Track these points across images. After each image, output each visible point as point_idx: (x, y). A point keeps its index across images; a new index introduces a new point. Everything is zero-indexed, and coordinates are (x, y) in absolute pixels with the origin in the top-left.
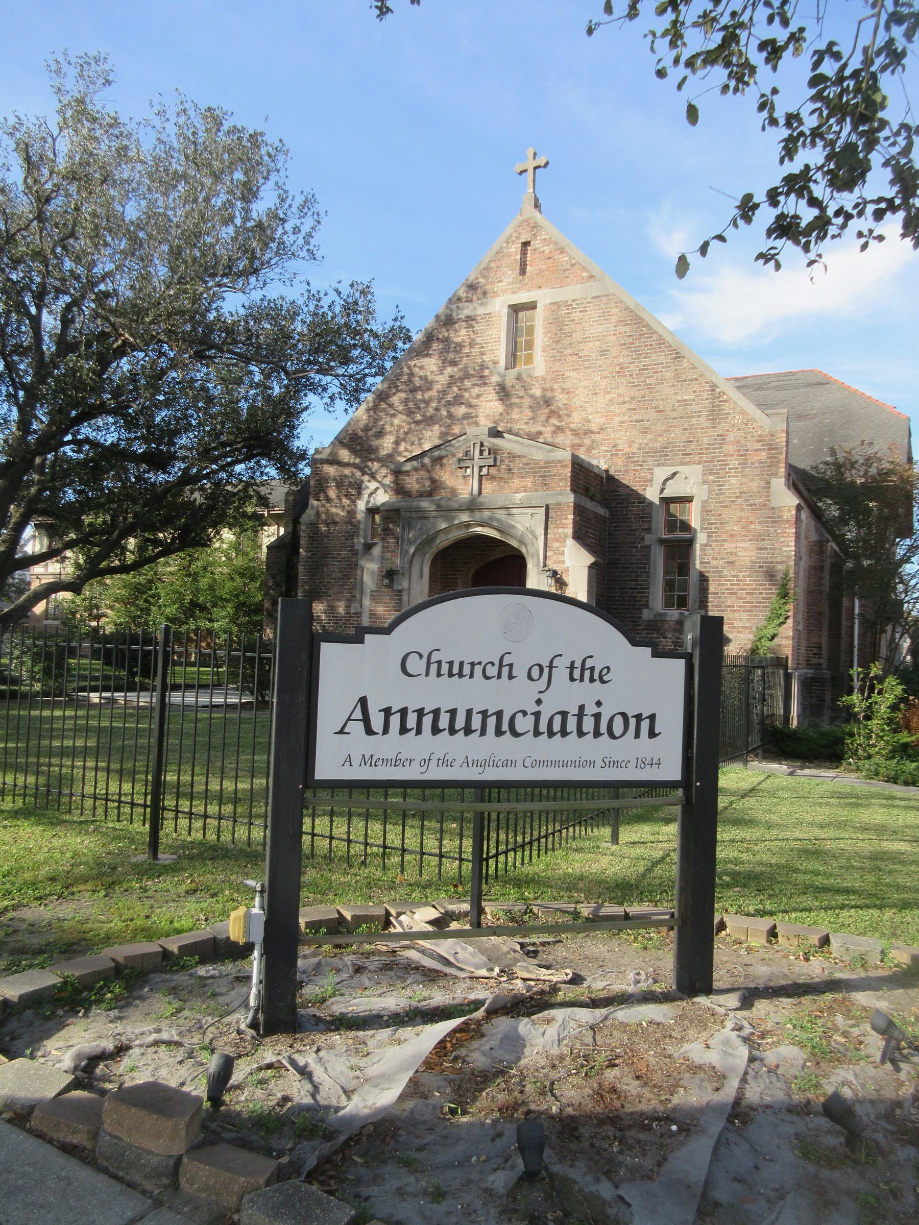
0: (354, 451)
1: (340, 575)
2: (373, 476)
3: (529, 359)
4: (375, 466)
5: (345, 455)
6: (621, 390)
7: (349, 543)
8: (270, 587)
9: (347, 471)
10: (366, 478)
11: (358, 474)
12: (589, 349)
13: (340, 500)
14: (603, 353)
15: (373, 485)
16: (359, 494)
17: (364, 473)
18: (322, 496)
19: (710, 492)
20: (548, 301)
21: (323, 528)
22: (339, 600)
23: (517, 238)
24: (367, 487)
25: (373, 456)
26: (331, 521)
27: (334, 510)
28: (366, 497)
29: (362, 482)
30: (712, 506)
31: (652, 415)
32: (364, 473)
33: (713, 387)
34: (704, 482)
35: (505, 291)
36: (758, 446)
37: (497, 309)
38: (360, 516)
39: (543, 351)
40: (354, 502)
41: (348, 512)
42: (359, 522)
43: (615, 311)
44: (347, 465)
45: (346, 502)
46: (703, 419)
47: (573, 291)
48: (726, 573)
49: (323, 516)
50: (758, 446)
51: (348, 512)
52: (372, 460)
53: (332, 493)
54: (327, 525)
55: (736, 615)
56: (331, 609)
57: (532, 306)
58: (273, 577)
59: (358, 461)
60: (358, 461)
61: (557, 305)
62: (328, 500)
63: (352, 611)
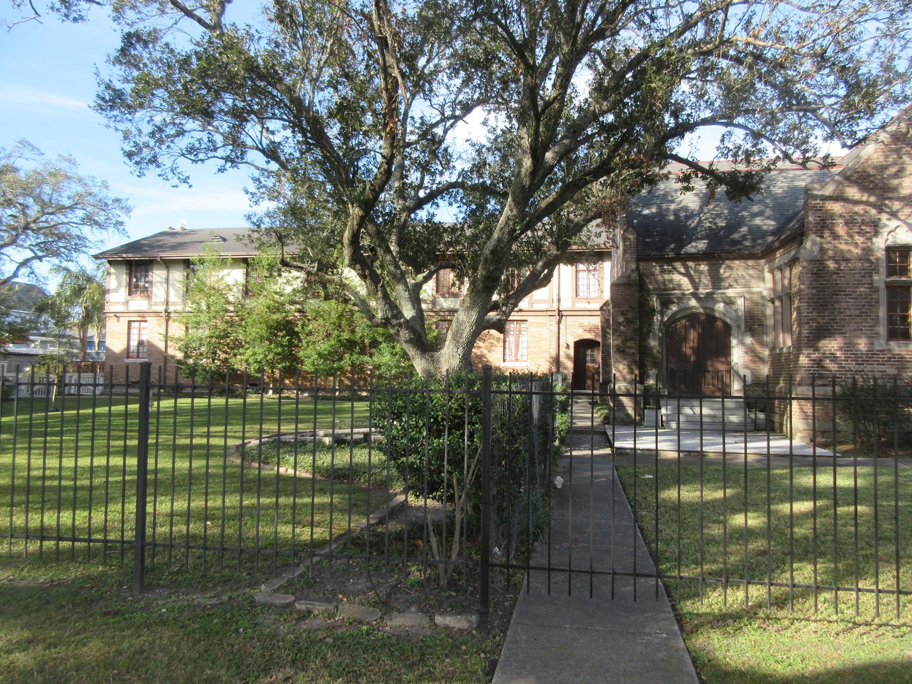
0: (864, 189)
1: (857, 312)
2: (894, 215)
4: (896, 205)
5: (853, 192)
7: (864, 280)
8: (620, 324)
9: (859, 209)
10: (884, 217)
11: (873, 212)
13: (852, 236)
15: (894, 223)
16: (876, 233)
17: (880, 210)
18: (827, 234)
21: (831, 265)
22: (858, 337)
24: (887, 226)
25: (891, 195)
26: (841, 258)
27: (843, 247)
28: (885, 237)
29: (879, 219)
32: (880, 210)
38: (881, 254)
40: (870, 239)
41: (863, 249)
42: (878, 259)
44: (857, 202)
45: (859, 239)
49: (830, 253)
51: (863, 249)
52: (890, 199)
53: (841, 230)
54: (836, 262)
56: (849, 347)
58: (623, 314)
59: (872, 199)
60: (872, 199)
62: (836, 236)
63: (877, 347)
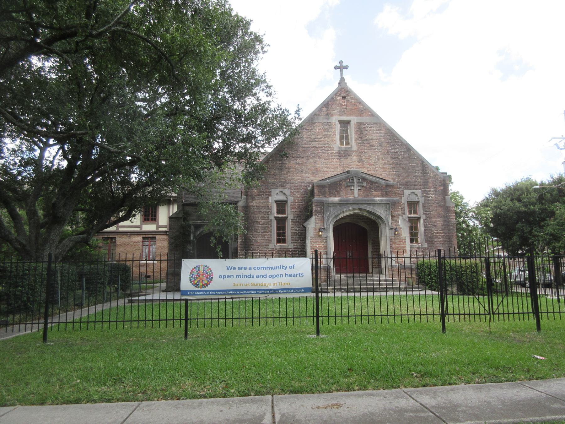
3: (347, 143)
6: (389, 160)
12: (375, 142)
14: (380, 145)
19: (425, 200)
20: (355, 122)
23: (340, 95)
30: (426, 205)
31: (401, 171)
33: (423, 162)
34: (423, 196)
35: (336, 115)
36: (440, 184)
37: (333, 121)
39: (355, 141)
43: (383, 129)
46: (420, 173)
47: (365, 119)
48: (433, 229)
50: (440, 184)
55: (438, 245)
57: (348, 122)
61: (359, 124)
